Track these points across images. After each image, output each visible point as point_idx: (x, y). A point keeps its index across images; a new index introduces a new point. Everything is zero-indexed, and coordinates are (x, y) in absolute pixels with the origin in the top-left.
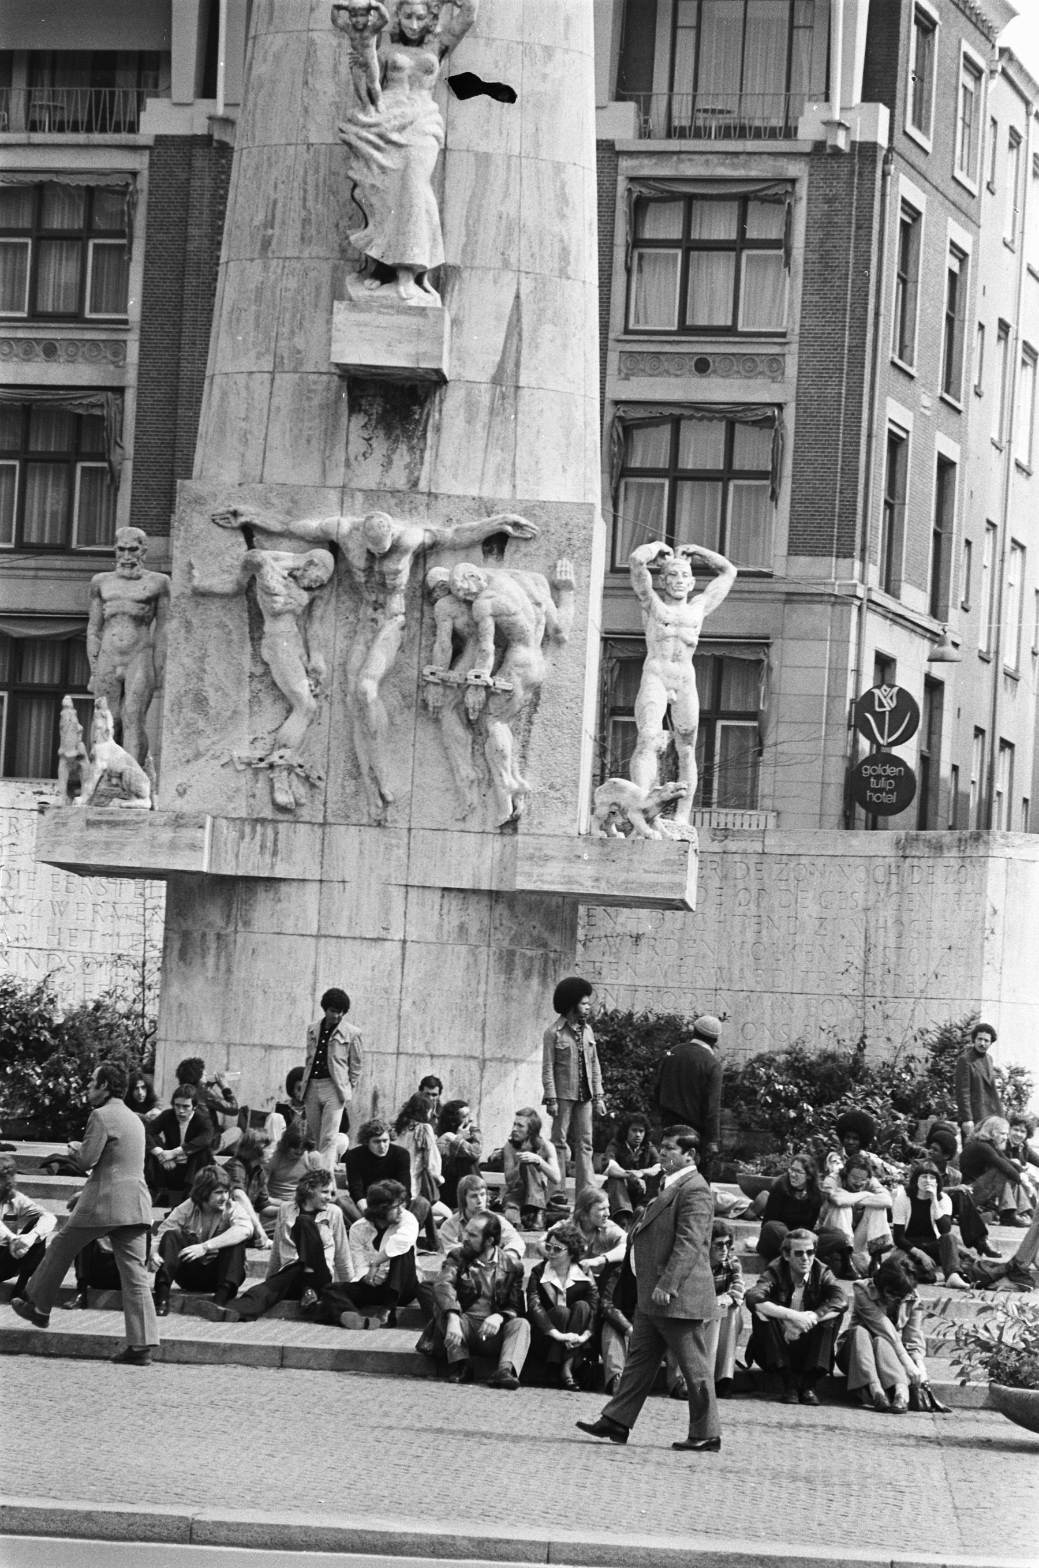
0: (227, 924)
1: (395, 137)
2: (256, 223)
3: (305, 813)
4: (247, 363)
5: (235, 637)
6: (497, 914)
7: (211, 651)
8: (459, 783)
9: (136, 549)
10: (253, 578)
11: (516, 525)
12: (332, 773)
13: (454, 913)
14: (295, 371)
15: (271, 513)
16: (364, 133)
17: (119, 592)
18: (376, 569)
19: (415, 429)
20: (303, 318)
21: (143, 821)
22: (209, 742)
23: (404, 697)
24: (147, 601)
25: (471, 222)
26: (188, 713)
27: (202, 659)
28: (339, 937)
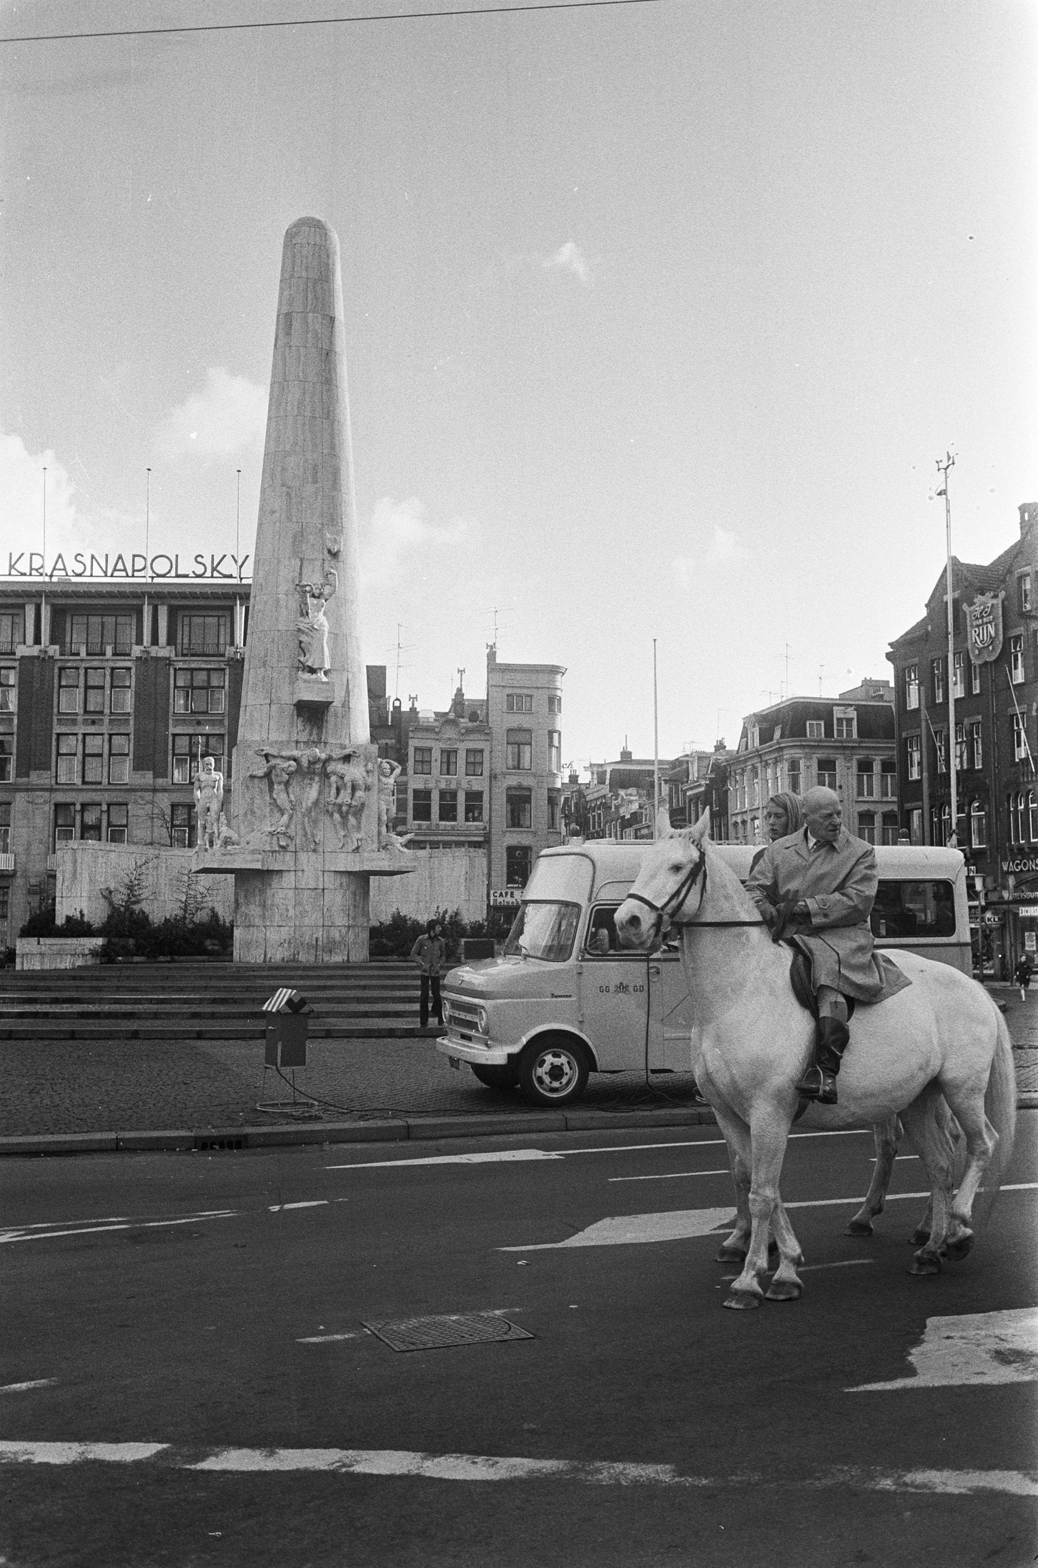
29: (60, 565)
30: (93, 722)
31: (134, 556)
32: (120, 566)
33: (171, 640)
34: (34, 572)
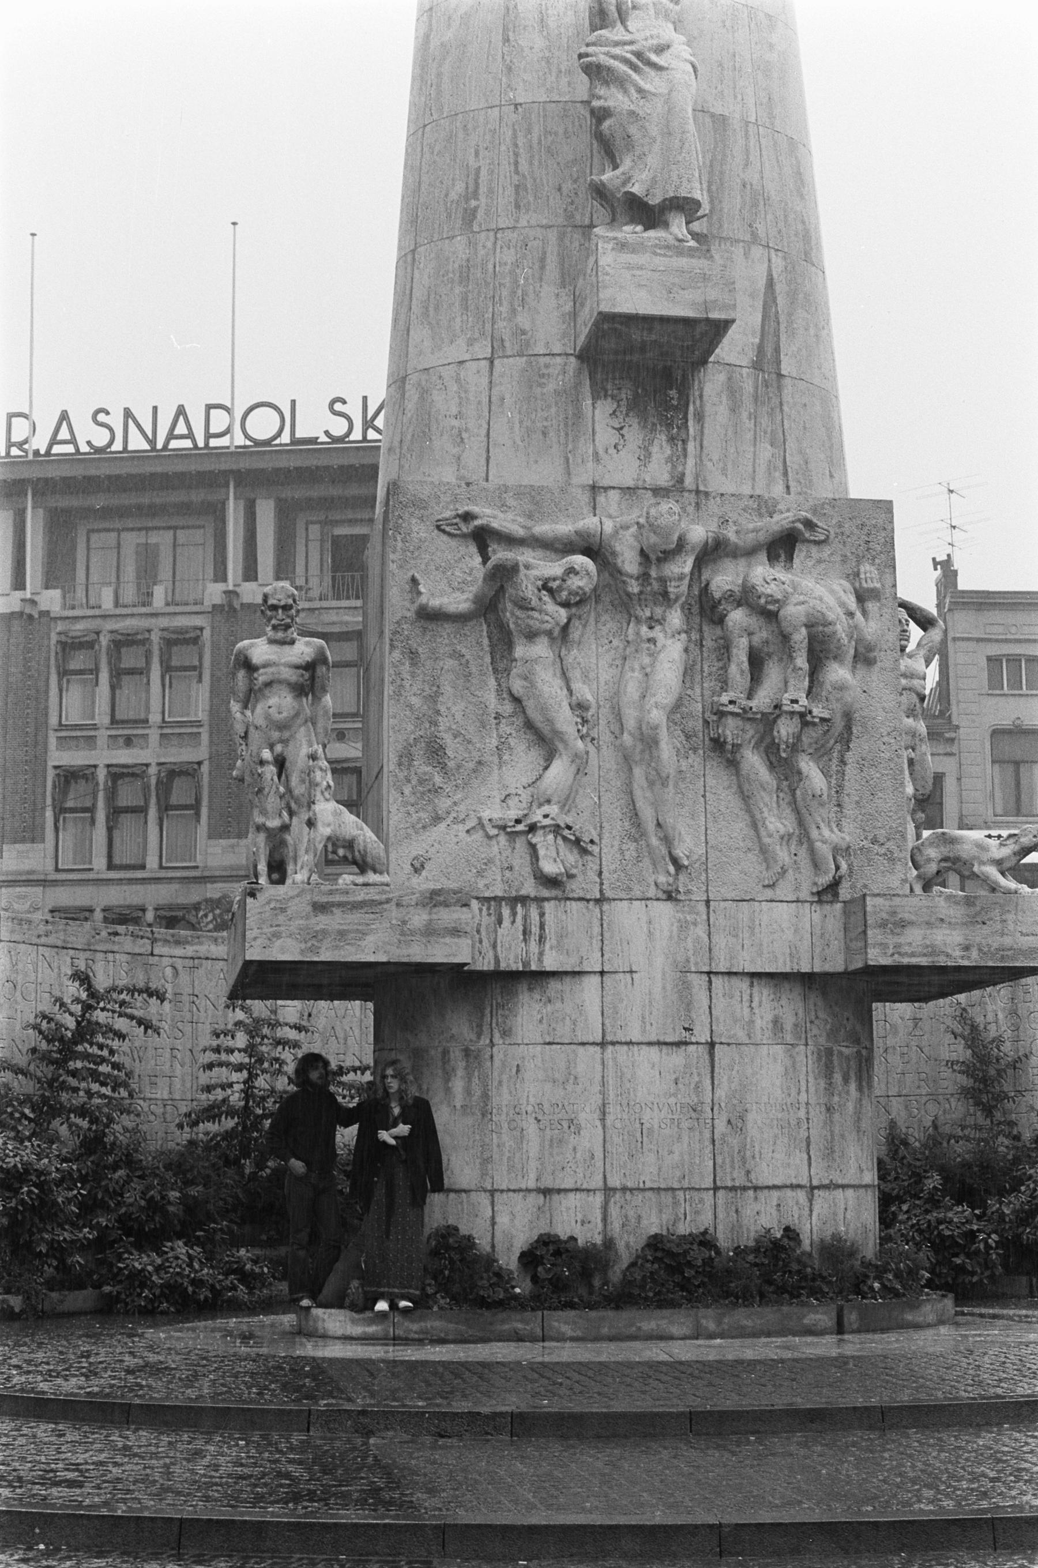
0: (479, 1035)
1: (654, 58)
2: (453, 196)
3: (575, 887)
4: (457, 351)
6: (811, 1002)
7: (447, 689)
8: (767, 840)
9: (291, 607)
11: (809, 524)
12: (606, 835)
13: (767, 1005)
14: (520, 355)
15: (510, 516)
16: (617, 51)
17: (273, 657)
18: (653, 573)
20: (525, 294)
21: (388, 901)
22: (449, 802)
23: (688, 737)
25: (714, 188)
26: (422, 767)
27: (432, 699)
28: (630, 1043)
29: (64, 434)
30: (129, 741)
31: (209, 407)
32: (181, 429)
33: (283, 569)
34: (15, 451)
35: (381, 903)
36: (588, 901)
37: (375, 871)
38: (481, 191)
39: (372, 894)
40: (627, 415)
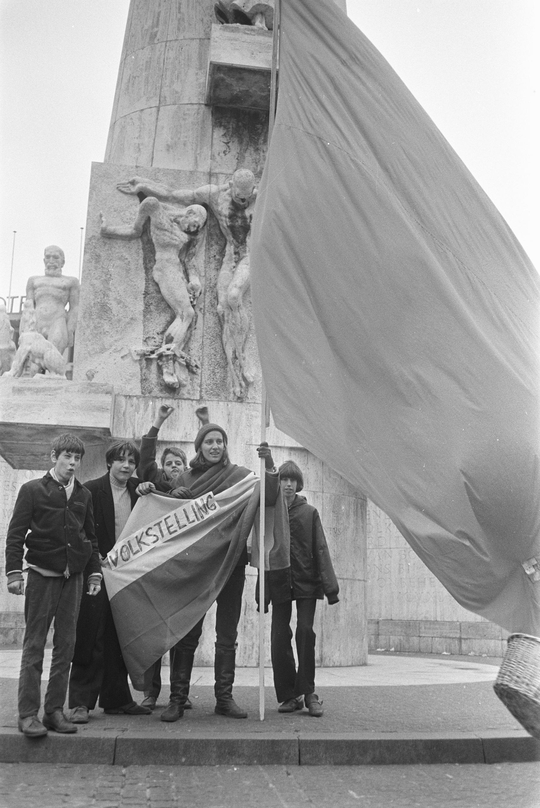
2: (146, 27)
5: (132, 267)
10: (149, 219)
14: (174, 104)
19: (258, 139)
20: (180, 73)
22: (112, 340)
24: (64, 289)
27: (107, 281)
35: (55, 390)
36: (192, 400)
37: (57, 373)
38: (160, 23)
39: (52, 384)
40: (232, 136)
